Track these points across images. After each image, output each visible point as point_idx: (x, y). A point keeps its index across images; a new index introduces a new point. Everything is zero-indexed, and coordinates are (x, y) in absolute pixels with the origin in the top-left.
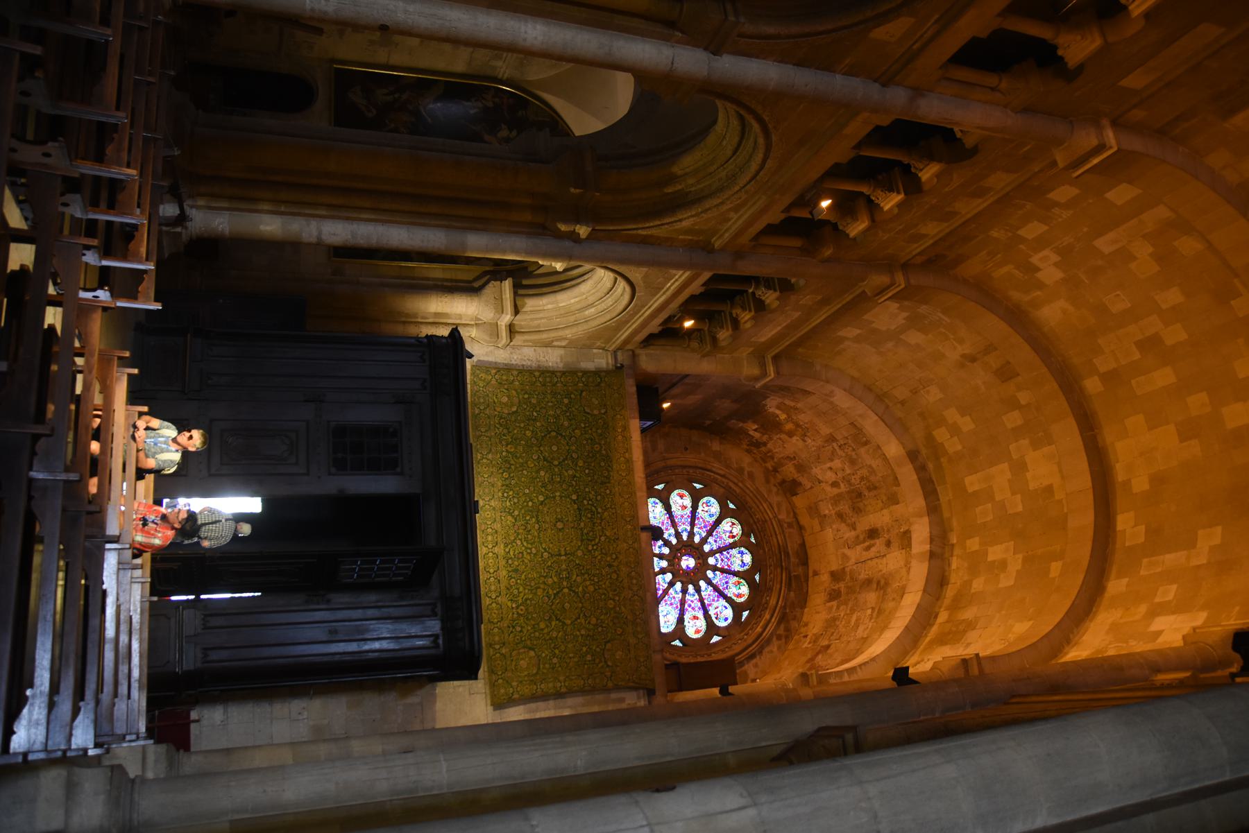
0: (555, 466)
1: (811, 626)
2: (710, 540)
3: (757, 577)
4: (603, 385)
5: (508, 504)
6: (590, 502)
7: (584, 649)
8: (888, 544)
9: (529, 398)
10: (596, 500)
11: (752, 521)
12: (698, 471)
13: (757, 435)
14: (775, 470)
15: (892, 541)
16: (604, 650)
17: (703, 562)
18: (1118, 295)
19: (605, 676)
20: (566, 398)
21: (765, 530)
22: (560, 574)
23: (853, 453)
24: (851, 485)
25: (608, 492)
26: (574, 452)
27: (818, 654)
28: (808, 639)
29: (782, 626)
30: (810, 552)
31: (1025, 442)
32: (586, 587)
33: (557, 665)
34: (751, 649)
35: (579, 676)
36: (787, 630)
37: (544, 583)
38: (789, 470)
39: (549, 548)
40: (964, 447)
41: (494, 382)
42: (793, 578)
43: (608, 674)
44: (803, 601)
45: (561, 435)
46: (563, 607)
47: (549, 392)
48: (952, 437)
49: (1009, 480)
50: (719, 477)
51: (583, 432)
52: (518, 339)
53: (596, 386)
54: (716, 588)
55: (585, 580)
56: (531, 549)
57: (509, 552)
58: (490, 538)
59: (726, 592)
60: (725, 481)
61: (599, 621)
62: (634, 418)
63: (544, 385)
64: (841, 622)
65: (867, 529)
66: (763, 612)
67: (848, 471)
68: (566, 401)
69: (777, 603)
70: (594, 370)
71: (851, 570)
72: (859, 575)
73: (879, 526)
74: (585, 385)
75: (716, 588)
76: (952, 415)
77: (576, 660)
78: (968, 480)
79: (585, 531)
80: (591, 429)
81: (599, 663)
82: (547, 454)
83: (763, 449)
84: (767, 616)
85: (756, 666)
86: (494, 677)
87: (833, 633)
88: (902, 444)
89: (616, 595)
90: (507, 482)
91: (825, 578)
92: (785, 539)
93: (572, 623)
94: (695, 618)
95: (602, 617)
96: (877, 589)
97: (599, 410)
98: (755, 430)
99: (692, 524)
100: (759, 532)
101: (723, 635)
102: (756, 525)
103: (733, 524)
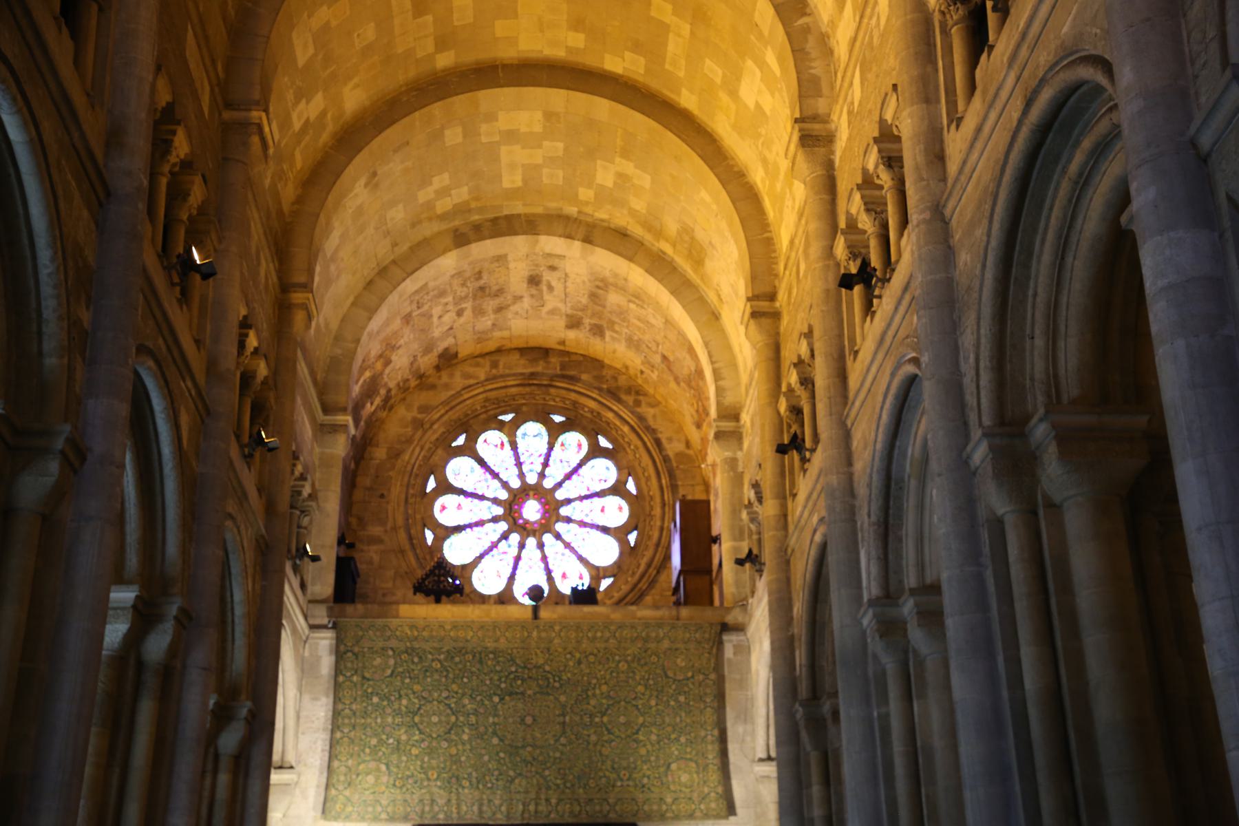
0: (457, 719)
1: (629, 363)
2: (503, 476)
3: (558, 419)
4: (356, 649)
5: (500, 783)
6: (503, 679)
7: (672, 703)
8: (553, 268)
9: (369, 747)
10: (501, 671)
12: (412, 482)
13: (378, 401)
14: (421, 377)
15: (550, 264)
16: (675, 680)
17: (533, 490)
18: (358, 35)
19: (703, 681)
20: (371, 699)
21: (497, 399)
22: (586, 725)
23: (432, 294)
24: (466, 297)
26: (440, 695)
27: (670, 370)
28: (647, 371)
29: (624, 397)
30: (532, 344)
31: (484, 128)
32: (602, 694)
33: (688, 737)
34: (649, 444)
35: (701, 712)
36: (629, 391)
37: (595, 745)
38: (427, 362)
39: (554, 736)
40: (467, 185)
41: (347, 793)
42: (564, 373)
43: (701, 677)
44: (595, 364)
45: (419, 709)
46: (624, 724)
47: (363, 721)
48: (450, 195)
49: (523, 148)
50: (422, 454)
51: (416, 680)
52: (291, 758)
53: (357, 658)
54: (568, 477)
55: (594, 695)
56: (555, 758)
57: (558, 785)
58: (540, 808)
59: (574, 464)
61: (642, 682)
62: (397, 611)
63: (354, 727)
64: (635, 334)
66: (604, 420)
67: (450, 299)
68: (375, 700)
69: (594, 399)
70: (333, 658)
71: (571, 309)
72: (580, 302)
73: (527, 274)
74: (356, 672)
75: (568, 477)
76: (424, 196)
77: (683, 714)
78: (506, 184)
79: (537, 689)
80: (413, 670)
81: (688, 687)
82: (441, 730)
83: (393, 393)
84: (610, 415)
85: (670, 440)
86: (698, 814)
87: (647, 346)
88: (445, 252)
90: (474, 780)
91: (571, 335)
92: (514, 375)
93: (642, 716)
94: (603, 510)
95: (638, 677)
96: (607, 291)
97: (389, 657)
98: (372, 404)
99: (482, 498)
101: (627, 475)
103: (485, 441)
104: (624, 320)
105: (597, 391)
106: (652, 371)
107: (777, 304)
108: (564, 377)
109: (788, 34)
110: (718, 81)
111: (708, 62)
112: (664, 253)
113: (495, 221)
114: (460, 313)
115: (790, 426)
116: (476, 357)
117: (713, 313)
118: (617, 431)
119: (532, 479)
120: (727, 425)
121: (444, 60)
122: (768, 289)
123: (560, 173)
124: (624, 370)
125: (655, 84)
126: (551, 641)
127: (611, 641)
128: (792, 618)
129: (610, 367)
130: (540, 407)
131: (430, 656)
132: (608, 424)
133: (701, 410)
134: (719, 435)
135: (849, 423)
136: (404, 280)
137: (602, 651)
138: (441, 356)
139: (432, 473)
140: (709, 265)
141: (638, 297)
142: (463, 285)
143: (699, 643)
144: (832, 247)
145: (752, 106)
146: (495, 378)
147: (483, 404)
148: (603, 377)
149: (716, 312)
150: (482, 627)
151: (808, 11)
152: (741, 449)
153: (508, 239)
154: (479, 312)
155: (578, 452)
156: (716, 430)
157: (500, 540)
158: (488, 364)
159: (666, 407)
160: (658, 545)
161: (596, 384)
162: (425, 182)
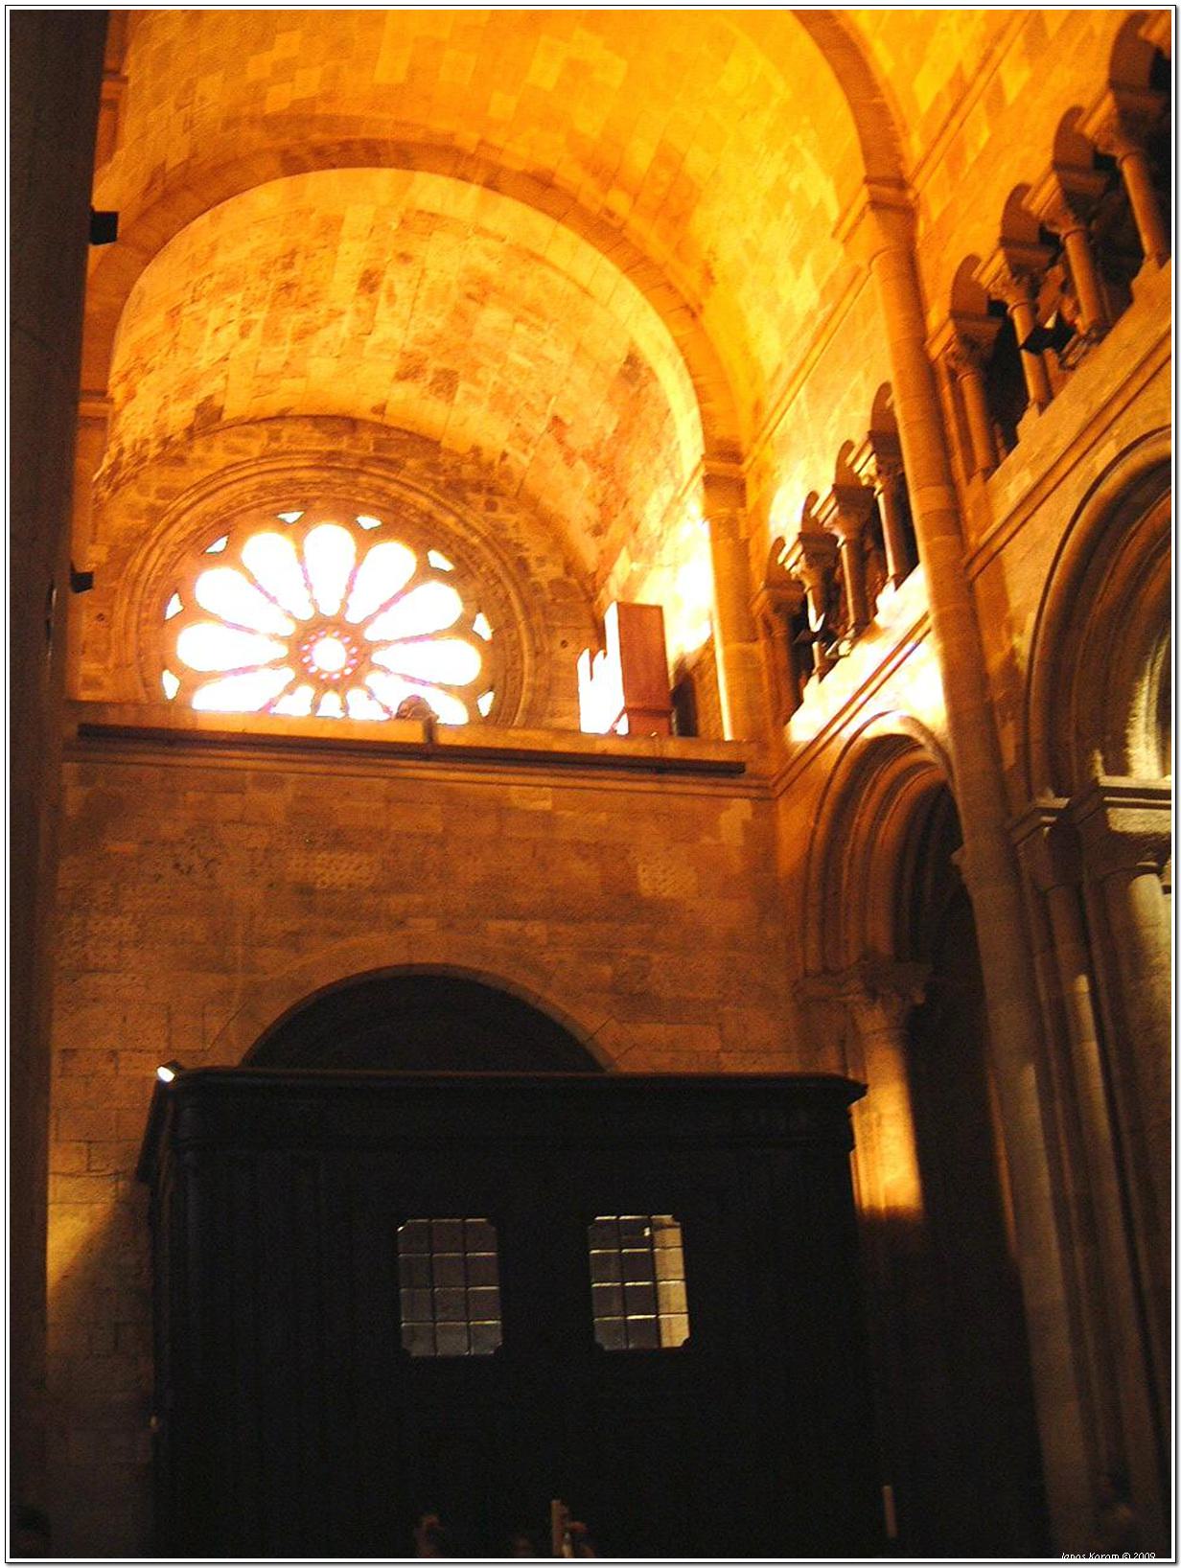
1: (485, 442)
8: (405, 258)
14: (165, 442)
23: (215, 279)
24: (262, 299)
27: (561, 442)
38: (181, 414)
42: (380, 454)
44: (427, 444)
60: (168, 551)
65: (354, 290)
83: (125, 457)
85: (541, 560)
88: (270, 177)
92: (304, 452)
100: (278, 501)
106: (525, 451)
107: (911, 195)
114: (244, 333)
115: (953, 375)
116: (247, 423)
129: (450, 452)
146: (277, 454)
147: (254, 493)
148: (440, 464)
152: (743, 504)
158: (266, 434)
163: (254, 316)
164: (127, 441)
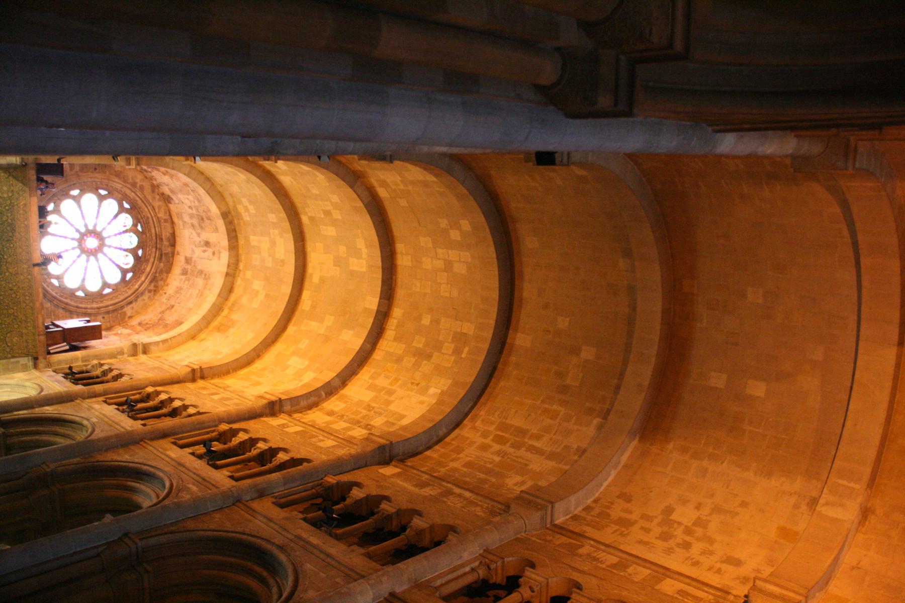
3: (140, 252)
8: (214, 253)
11: (139, 217)
15: (215, 252)
21: (149, 223)
24: (198, 211)
25: (12, 245)
29: (153, 285)
30: (178, 239)
31: (276, 231)
34: (129, 298)
43: (8, 350)
44: (169, 269)
61: (3, 322)
62: (34, 196)
65: (205, 239)
66: (141, 275)
69: (151, 270)
72: (198, 265)
73: (211, 241)
78: (252, 238)
83: (150, 174)
84: (143, 278)
85: (132, 308)
87: (178, 298)
88: (219, 208)
89: (15, 306)
92: (161, 230)
95: (5, 319)
97: (8, 194)
102: (143, 220)
104: (190, 286)
105: (155, 271)
106: (166, 299)
107: (199, 380)
108: (161, 255)
109: (317, 389)
110: (299, 346)
111: (307, 341)
112: (222, 311)
113: (235, 230)
114: (190, 207)
115: (140, 393)
116: (169, 212)
117: (195, 336)
118: (135, 282)
119: (107, 242)
120: (140, 348)
121: (305, 219)
122: (206, 375)
123: (258, 263)
124: (166, 283)
125: (297, 314)
126: (22, 274)
127: (24, 304)
128: (43, 406)
129: (167, 277)
130: (145, 244)
131: (10, 215)
132: (139, 277)
133: (148, 326)
134: (135, 345)
135: (141, 443)
136: (204, 189)
137: (19, 300)
138: (169, 196)
139: (109, 193)
140: (217, 335)
141: (201, 294)
142: (204, 211)
143: (26, 347)
144: (224, 422)
145: (289, 363)
146: (159, 222)
148: (162, 274)
149: (195, 338)
150: (27, 240)
151: (327, 396)
152: (128, 356)
153: (226, 237)
154: (191, 216)
155: (124, 264)
156: (137, 344)
157: (75, 228)
159: (149, 305)
160: (77, 307)
161: (158, 271)
162: (251, 202)
163: (194, 210)
164: (153, 174)
